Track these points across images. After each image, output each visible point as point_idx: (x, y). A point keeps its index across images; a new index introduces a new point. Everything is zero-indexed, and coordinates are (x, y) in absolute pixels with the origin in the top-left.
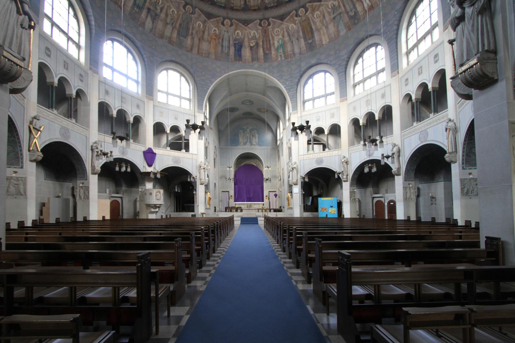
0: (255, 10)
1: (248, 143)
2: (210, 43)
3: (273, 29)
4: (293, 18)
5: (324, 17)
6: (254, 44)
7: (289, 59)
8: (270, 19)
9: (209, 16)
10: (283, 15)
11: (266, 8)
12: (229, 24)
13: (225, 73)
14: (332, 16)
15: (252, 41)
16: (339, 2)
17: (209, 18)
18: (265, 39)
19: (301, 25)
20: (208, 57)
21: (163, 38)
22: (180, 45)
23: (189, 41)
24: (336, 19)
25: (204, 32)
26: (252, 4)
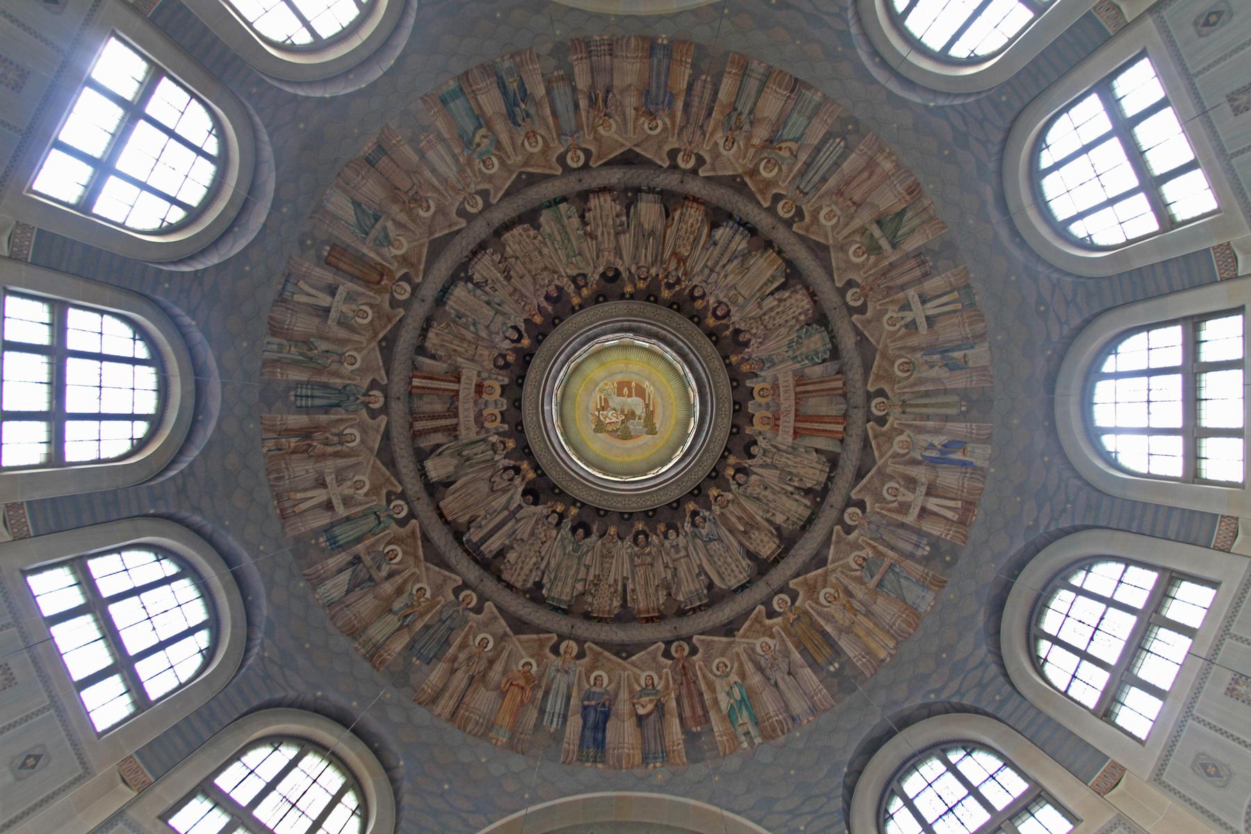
0: (649, 620)
2: (503, 694)
3: (708, 660)
4: (760, 623)
5: (849, 594)
6: (650, 707)
7: (782, 739)
8: (695, 639)
9: (519, 626)
10: (731, 622)
11: (681, 613)
12: (574, 654)
14: (873, 583)
15: (644, 700)
16: (874, 548)
17: (517, 631)
18: (684, 691)
19: (789, 634)
20: (484, 736)
21: (355, 639)
22: (401, 678)
23: (436, 675)
24: (886, 583)
25: (491, 662)
26: (642, 605)
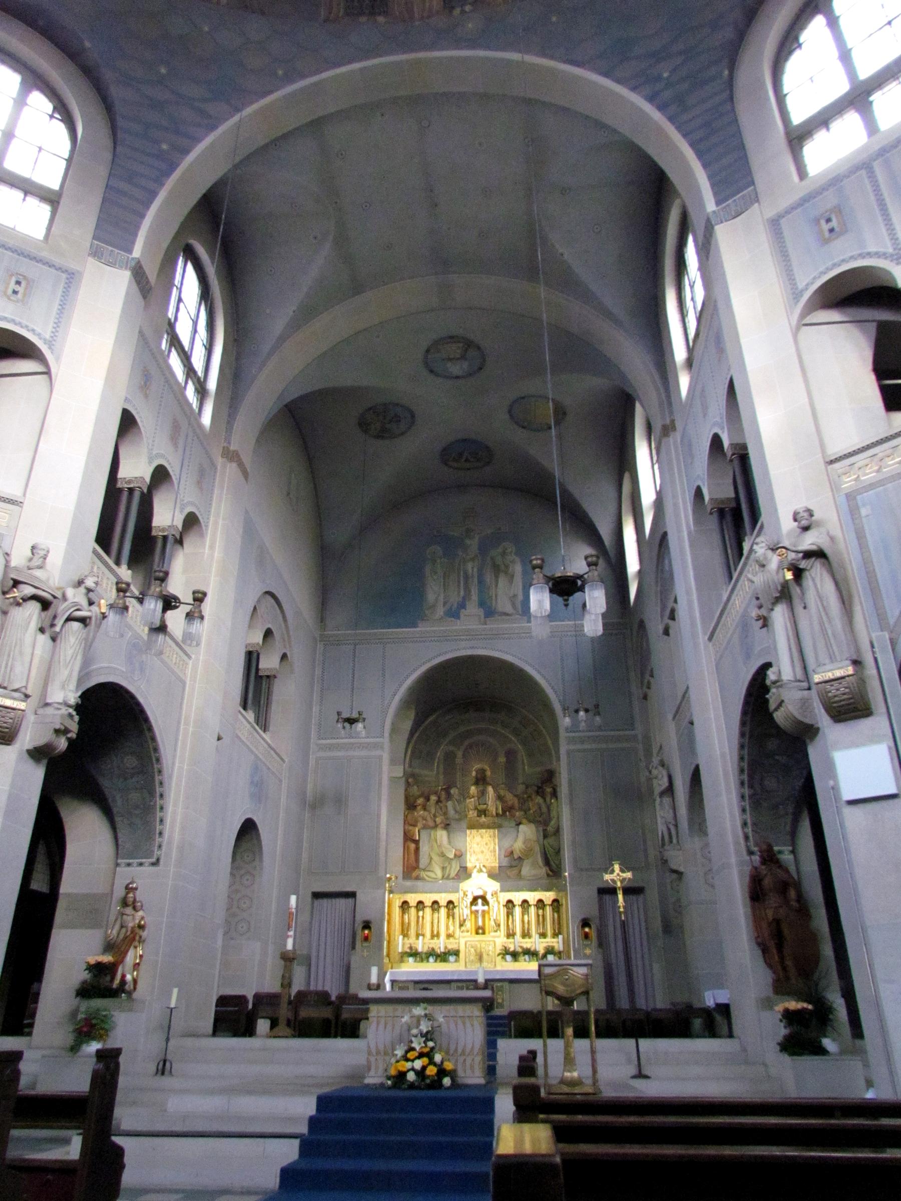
1: (473, 609)
13: (289, 78)
